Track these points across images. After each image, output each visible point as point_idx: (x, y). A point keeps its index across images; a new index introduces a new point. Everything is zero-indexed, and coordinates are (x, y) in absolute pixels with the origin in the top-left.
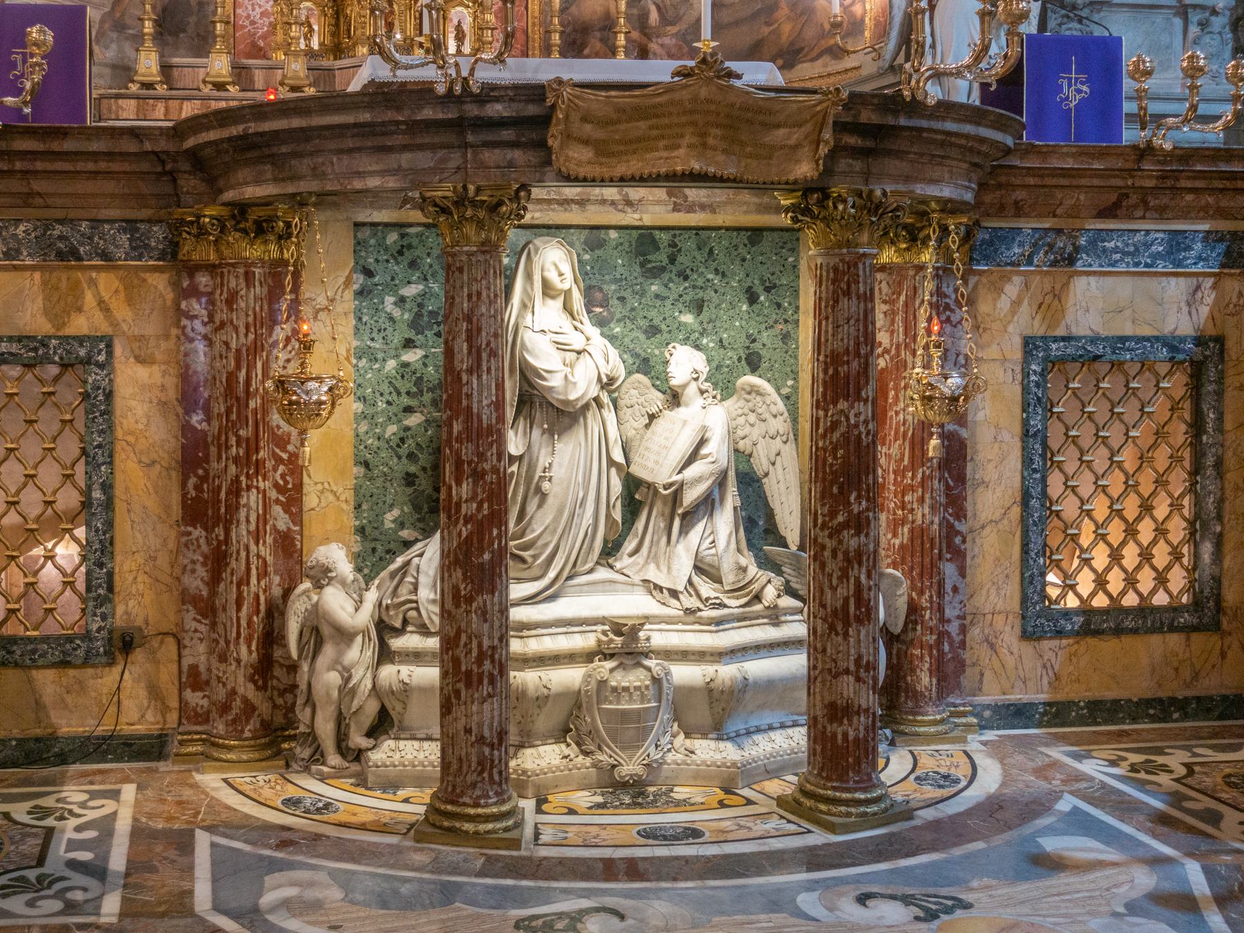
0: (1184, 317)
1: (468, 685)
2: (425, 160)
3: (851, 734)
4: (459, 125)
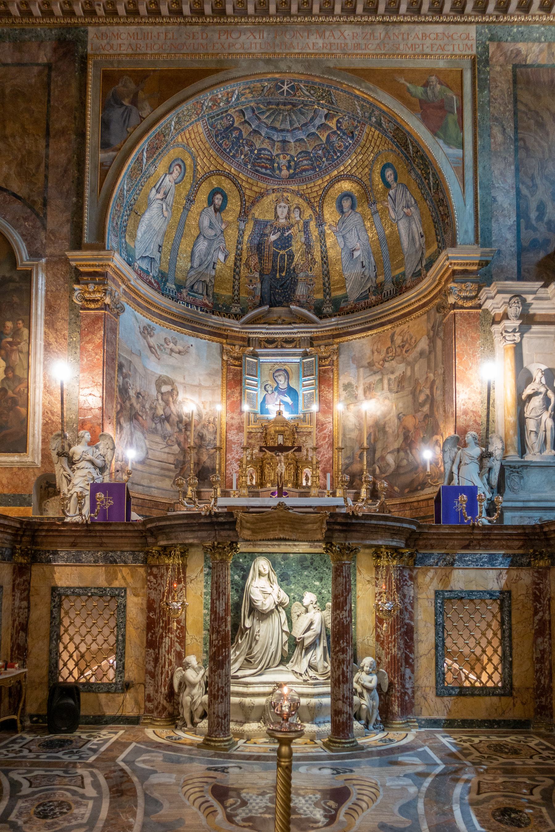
0: (496, 584)
1: (214, 699)
2: (204, 534)
3: (341, 720)
4: (212, 524)
